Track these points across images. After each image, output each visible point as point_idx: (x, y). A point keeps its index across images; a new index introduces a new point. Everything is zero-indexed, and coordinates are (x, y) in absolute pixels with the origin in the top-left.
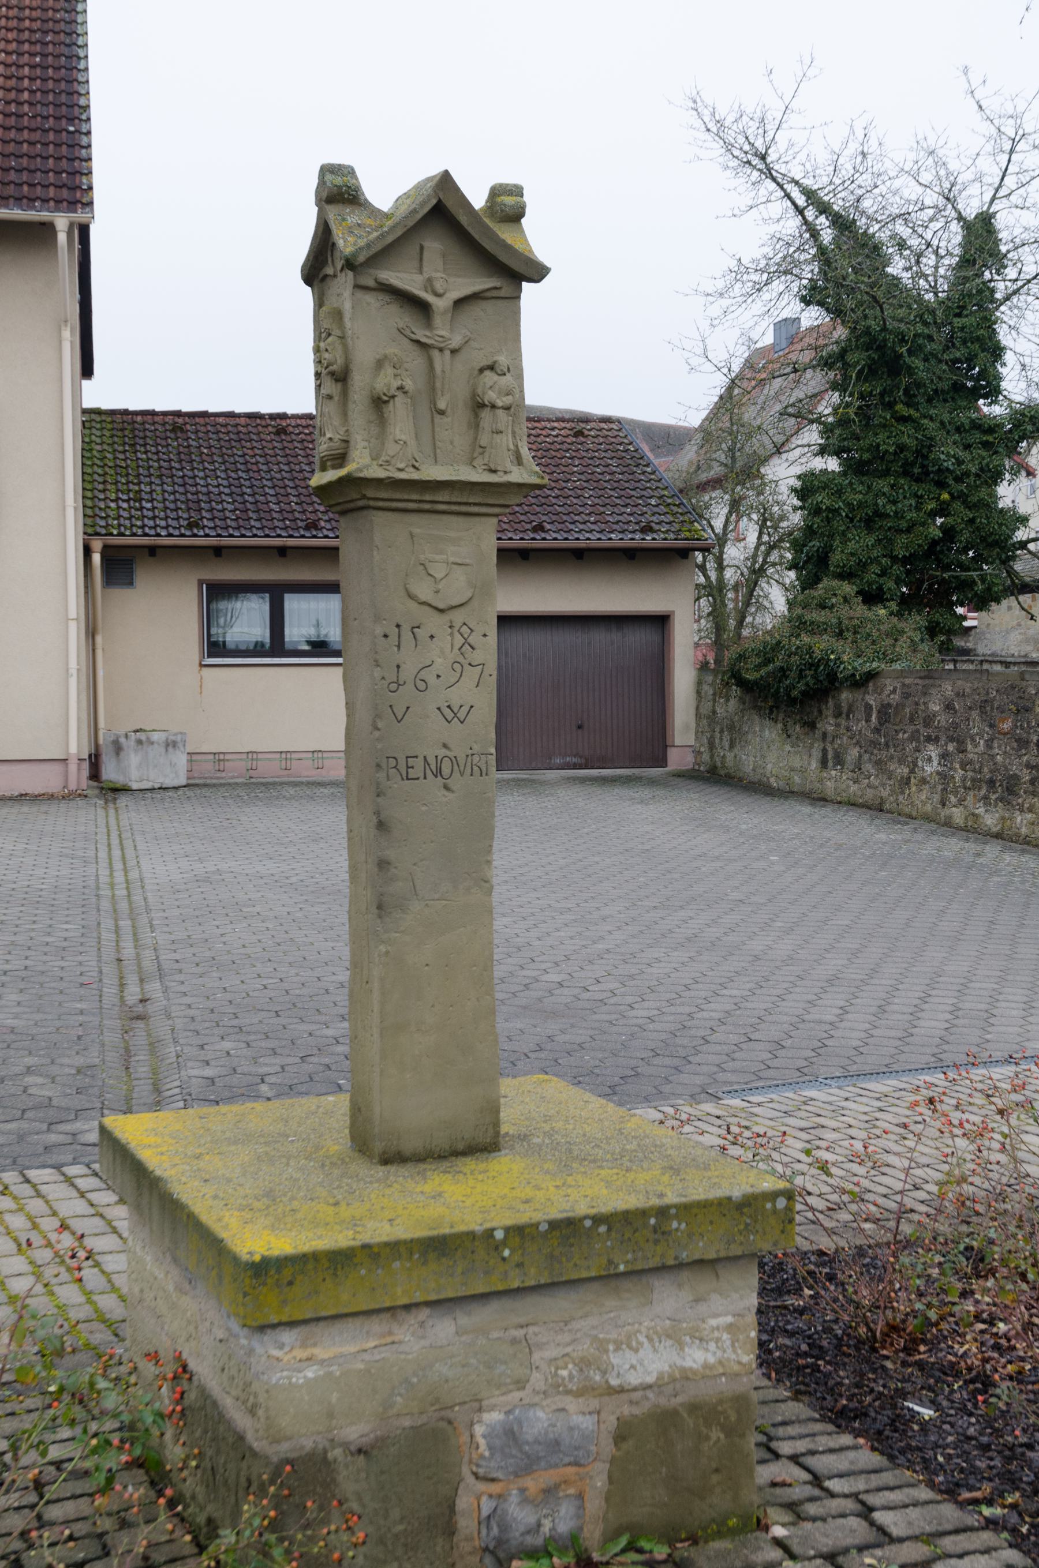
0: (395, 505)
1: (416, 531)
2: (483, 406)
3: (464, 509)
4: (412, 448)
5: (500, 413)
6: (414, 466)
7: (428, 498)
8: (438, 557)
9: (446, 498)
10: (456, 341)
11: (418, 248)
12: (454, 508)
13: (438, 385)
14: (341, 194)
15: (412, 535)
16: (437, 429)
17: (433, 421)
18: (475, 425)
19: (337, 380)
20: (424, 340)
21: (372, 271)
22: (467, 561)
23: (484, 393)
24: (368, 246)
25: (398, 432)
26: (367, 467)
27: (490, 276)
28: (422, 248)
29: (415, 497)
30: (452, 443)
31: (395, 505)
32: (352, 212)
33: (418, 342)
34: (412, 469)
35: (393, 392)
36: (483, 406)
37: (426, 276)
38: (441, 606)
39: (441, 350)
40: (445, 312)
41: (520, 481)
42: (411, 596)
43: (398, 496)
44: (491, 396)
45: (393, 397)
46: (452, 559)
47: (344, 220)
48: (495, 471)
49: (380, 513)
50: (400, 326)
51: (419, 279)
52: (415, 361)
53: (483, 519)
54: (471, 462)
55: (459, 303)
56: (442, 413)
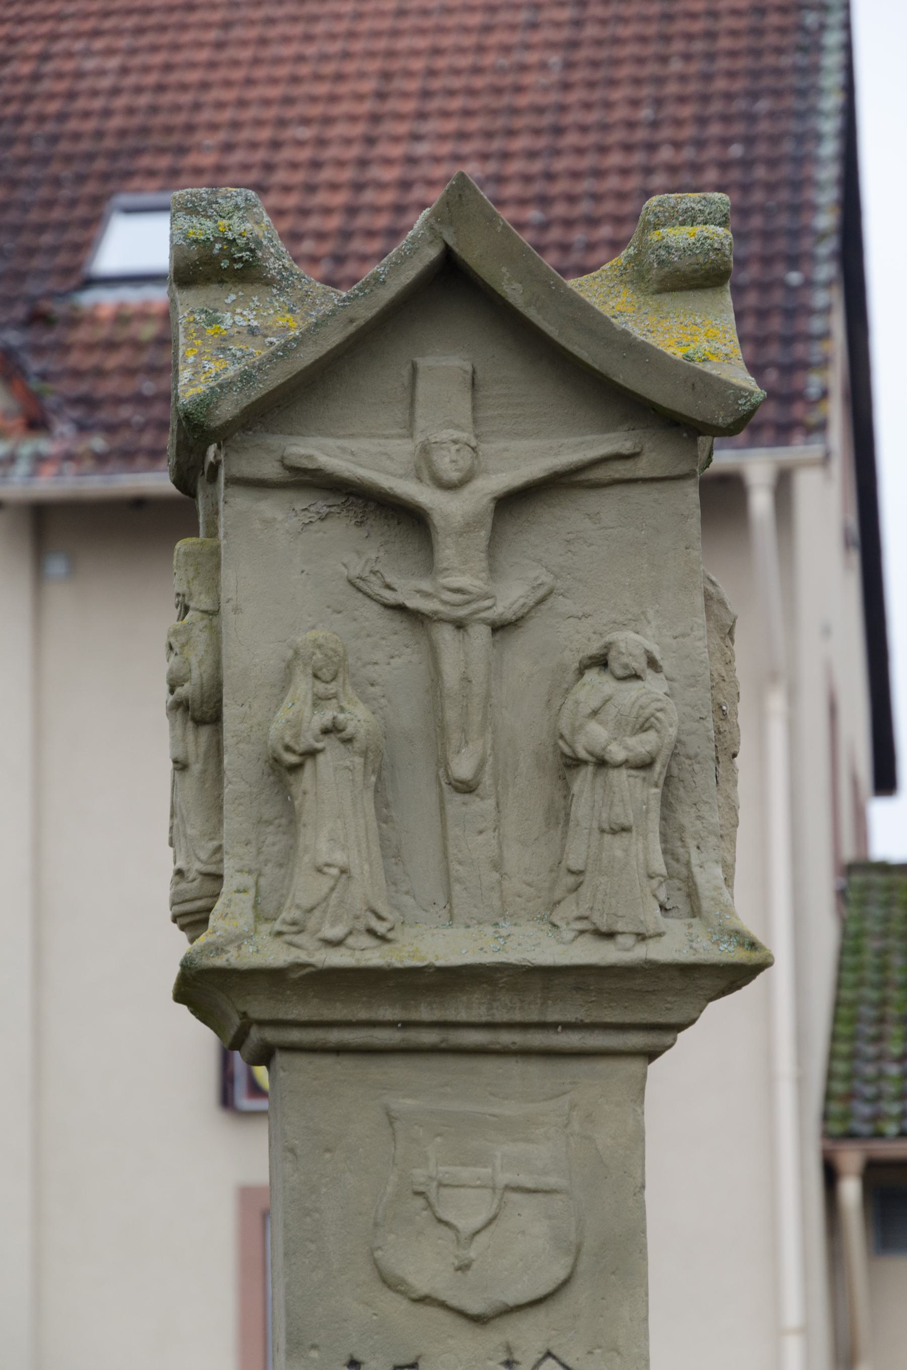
0: (335, 1037)
1: (403, 1103)
2: (573, 763)
3: (537, 1039)
4: (366, 887)
5: (621, 778)
6: (371, 932)
7: (425, 1014)
8: (466, 1174)
9: (479, 1014)
10: (509, 598)
11: (406, 372)
12: (506, 1038)
13: (451, 715)
14: (209, 261)
15: (391, 1119)
16: (454, 832)
17: (442, 809)
18: (559, 816)
19: (199, 722)
20: (414, 603)
21: (275, 441)
22: (552, 1181)
23: (575, 730)
24: (246, 377)
25: (323, 845)
26: (238, 940)
27: (608, 428)
28: (414, 370)
29: (387, 1013)
30: (497, 865)
31: (335, 1037)
32: (243, 302)
33: (400, 608)
34: (367, 941)
35: (308, 741)
36: (573, 763)
37: (419, 438)
38: (475, 1307)
39: (460, 625)
40: (468, 528)
41: (685, 956)
42: (391, 1283)
43: (338, 1012)
44: (596, 735)
45: (312, 753)
46: (505, 1178)
47: (213, 321)
48: (610, 935)
49: (300, 1061)
50: (357, 568)
51: (403, 449)
52: (392, 657)
53: (602, 1065)
54: (547, 915)
55: (513, 503)
56: (466, 788)
